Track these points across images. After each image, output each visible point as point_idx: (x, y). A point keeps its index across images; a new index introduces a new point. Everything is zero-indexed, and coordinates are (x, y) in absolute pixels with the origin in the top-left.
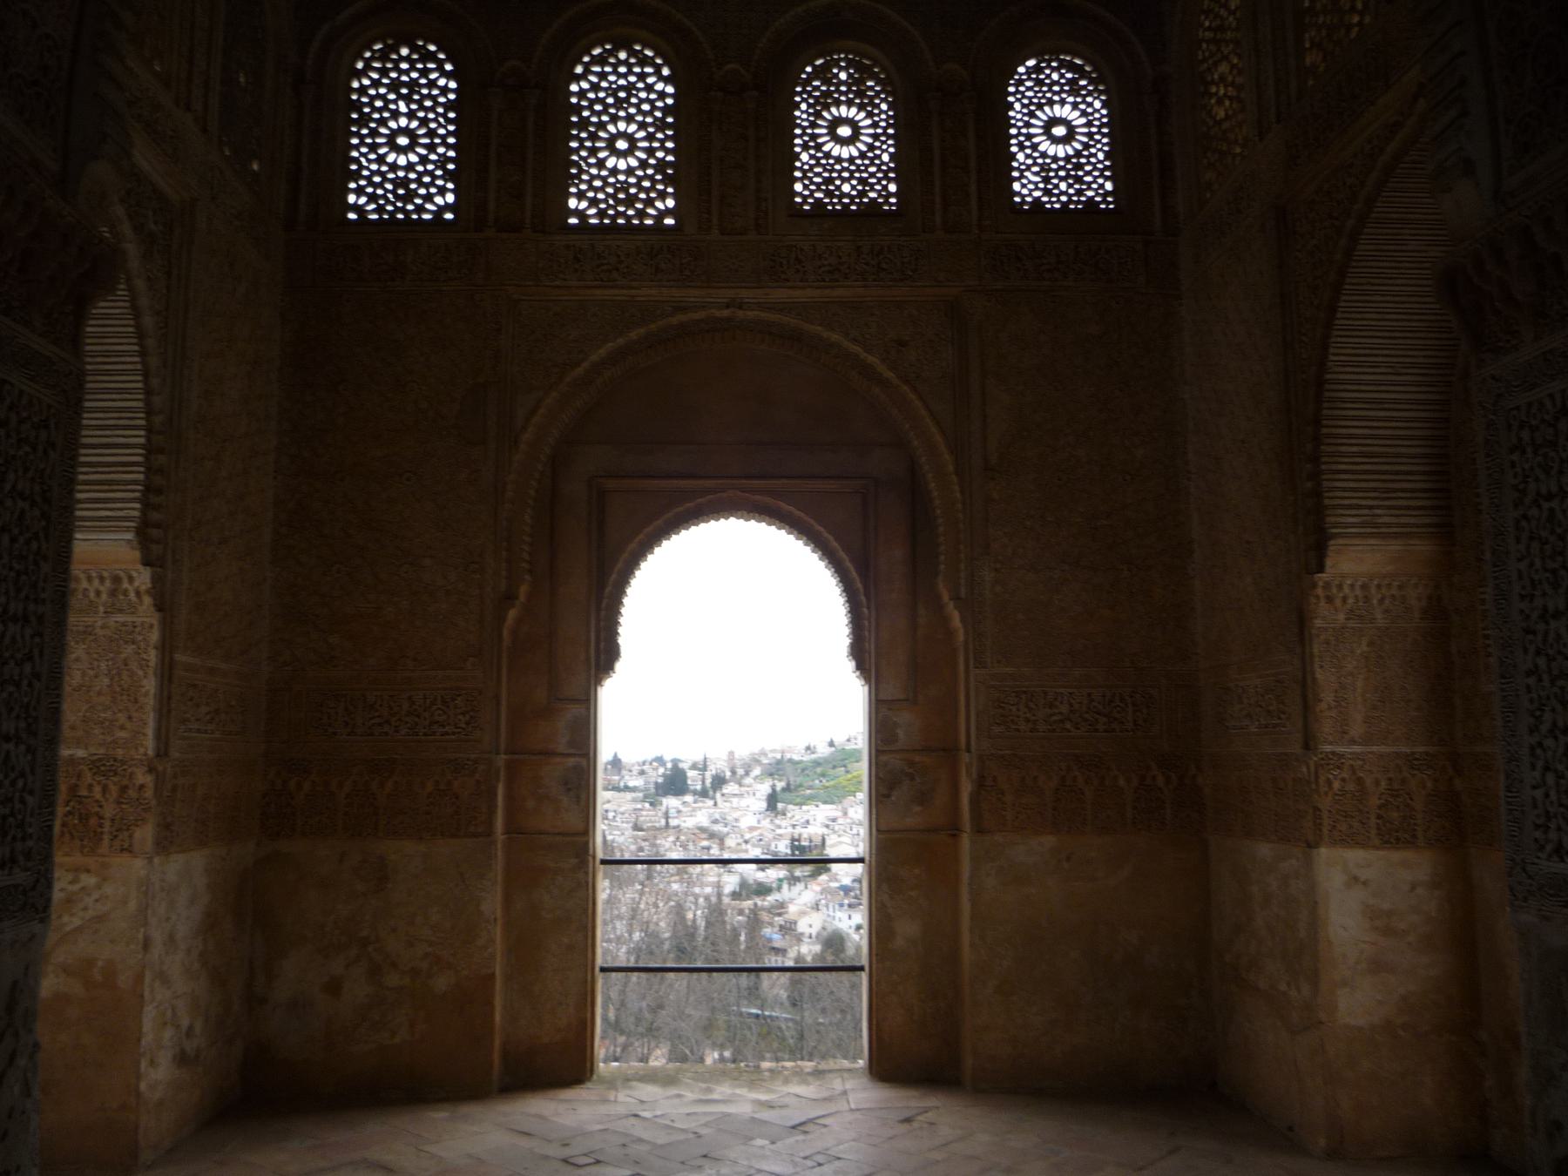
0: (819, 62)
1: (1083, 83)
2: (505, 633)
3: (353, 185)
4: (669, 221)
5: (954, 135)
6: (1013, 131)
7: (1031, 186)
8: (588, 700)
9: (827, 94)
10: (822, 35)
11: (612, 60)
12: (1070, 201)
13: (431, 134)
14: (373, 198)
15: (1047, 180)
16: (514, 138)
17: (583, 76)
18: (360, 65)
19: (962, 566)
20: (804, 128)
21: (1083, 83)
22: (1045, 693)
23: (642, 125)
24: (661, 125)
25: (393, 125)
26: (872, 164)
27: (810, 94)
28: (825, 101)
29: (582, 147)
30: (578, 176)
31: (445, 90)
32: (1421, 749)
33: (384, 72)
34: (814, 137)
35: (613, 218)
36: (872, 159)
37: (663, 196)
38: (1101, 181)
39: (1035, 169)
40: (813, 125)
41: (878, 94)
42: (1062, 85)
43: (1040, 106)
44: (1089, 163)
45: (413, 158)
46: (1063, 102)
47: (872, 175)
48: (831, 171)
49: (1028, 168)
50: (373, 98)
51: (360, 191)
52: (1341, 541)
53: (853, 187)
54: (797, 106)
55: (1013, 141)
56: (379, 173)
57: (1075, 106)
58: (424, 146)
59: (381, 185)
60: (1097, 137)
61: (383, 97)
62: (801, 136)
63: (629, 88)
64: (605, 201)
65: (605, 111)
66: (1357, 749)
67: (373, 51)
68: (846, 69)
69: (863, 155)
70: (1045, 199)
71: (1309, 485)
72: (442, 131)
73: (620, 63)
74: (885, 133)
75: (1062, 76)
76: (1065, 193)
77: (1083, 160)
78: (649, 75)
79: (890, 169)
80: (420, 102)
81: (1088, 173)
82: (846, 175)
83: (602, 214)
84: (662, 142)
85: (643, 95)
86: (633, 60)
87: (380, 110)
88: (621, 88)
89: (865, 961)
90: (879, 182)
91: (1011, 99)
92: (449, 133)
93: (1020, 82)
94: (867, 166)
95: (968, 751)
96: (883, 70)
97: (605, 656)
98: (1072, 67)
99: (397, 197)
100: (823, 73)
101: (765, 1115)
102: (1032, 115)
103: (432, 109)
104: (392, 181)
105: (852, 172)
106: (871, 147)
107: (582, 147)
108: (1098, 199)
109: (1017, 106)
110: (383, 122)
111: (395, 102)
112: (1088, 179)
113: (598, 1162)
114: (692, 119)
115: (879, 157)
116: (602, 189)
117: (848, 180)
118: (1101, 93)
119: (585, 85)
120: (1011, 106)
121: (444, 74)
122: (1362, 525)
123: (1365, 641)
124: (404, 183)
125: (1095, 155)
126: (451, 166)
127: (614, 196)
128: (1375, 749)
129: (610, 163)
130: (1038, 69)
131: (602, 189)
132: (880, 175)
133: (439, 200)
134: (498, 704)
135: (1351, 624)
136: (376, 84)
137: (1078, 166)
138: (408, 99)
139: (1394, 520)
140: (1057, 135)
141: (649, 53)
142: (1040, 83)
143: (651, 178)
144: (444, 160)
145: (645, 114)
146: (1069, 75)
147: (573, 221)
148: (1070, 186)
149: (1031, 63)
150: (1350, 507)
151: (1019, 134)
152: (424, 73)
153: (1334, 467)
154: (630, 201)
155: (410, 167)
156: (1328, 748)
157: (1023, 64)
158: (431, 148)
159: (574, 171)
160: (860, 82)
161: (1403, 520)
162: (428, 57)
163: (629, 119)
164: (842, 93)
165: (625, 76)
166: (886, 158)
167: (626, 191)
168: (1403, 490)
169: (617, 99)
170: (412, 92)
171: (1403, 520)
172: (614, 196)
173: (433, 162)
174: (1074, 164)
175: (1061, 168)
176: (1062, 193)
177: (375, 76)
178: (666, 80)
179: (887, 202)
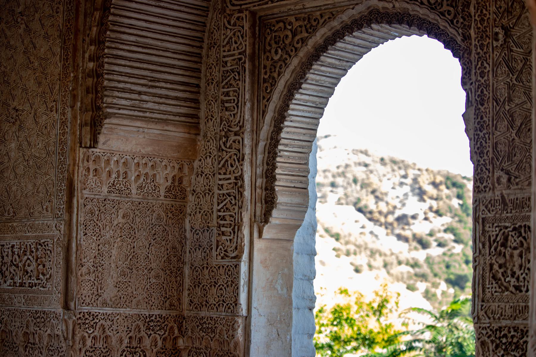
32: (157, 312)
52: (114, 121)
66: (109, 310)
71: (91, 65)
122: (133, 108)
123: (121, 213)
128: (122, 310)
135: (112, 197)
139: (157, 107)
150: (123, 90)
153: (115, 52)
156: (86, 309)
161: (163, 108)
168: (166, 81)
171: (163, 108)
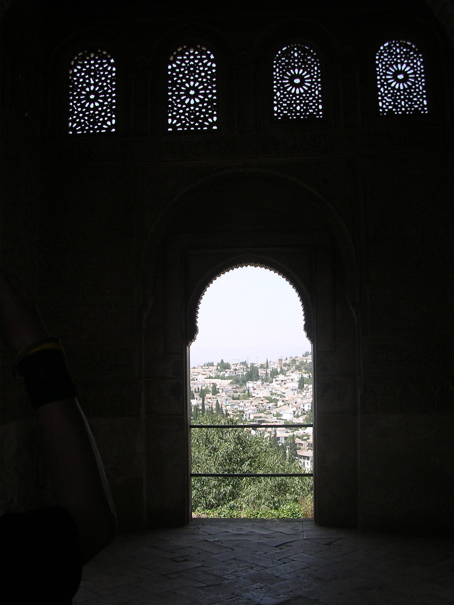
0: (284, 49)
1: (412, 53)
4: (215, 128)
5: (349, 82)
7: (387, 104)
9: (288, 64)
11: (187, 53)
12: (406, 110)
15: (395, 101)
16: (143, 92)
18: (73, 63)
20: (277, 81)
21: (412, 53)
23: (201, 83)
26: (311, 96)
28: (288, 67)
29: (173, 95)
30: (172, 108)
31: (111, 72)
33: (83, 66)
35: (189, 127)
36: (310, 94)
37: (211, 116)
38: (421, 100)
39: (389, 95)
40: (282, 79)
42: (402, 55)
43: (391, 65)
44: (415, 92)
45: (97, 104)
46: (402, 63)
48: (291, 101)
49: (386, 95)
50: (79, 78)
53: (301, 108)
54: (274, 70)
55: (379, 82)
56: (81, 112)
57: (408, 65)
60: (419, 79)
62: (276, 84)
63: (195, 66)
64: (184, 119)
65: (184, 77)
67: (78, 57)
68: (297, 51)
69: (306, 92)
70: (394, 110)
72: (110, 91)
74: (316, 81)
75: (401, 50)
77: (412, 91)
80: (100, 78)
81: (416, 97)
82: (298, 102)
83: (183, 126)
84: (211, 90)
85: (201, 69)
88: (191, 66)
90: (314, 105)
91: (377, 62)
92: (113, 92)
93: (382, 54)
94: (308, 97)
97: (191, 332)
98: (406, 46)
99: (90, 123)
100: (286, 54)
101: (264, 540)
105: (301, 101)
106: (310, 88)
108: (420, 109)
109: (380, 65)
110: (83, 89)
111: (89, 79)
112: (415, 99)
113: (186, 560)
114: (223, 78)
115: (314, 92)
116: (183, 114)
117: (299, 104)
118: (420, 58)
119: (174, 66)
120: (377, 66)
124: (93, 116)
125: (418, 88)
126: (114, 107)
127: (189, 117)
129: (187, 101)
130: (389, 47)
131: (183, 114)
132: (314, 101)
137: (410, 93)
138: (94, 77)
140: (400, 78)
142: (390, 54)
143: (206, 108)
145: (203, 77)
146: (405, 50)
147: (170, 129)
148: (406, 103)
149: (386, 45)
151: (381, 79)
154: (196, 119)
155: (95, 108)
158: (105, 99)
159: (170, 106)
160: (304, 57)
163: (195, 80)
164: (295, 63)
165: (193, 60)
166: (317, 93)
167: (194, 114)
169: (189, 71)
172: (189, 117)
173: (106, 106)
175: (401, 95)
176: (402, 107)
177: (79, 67)
178: (212, 61)
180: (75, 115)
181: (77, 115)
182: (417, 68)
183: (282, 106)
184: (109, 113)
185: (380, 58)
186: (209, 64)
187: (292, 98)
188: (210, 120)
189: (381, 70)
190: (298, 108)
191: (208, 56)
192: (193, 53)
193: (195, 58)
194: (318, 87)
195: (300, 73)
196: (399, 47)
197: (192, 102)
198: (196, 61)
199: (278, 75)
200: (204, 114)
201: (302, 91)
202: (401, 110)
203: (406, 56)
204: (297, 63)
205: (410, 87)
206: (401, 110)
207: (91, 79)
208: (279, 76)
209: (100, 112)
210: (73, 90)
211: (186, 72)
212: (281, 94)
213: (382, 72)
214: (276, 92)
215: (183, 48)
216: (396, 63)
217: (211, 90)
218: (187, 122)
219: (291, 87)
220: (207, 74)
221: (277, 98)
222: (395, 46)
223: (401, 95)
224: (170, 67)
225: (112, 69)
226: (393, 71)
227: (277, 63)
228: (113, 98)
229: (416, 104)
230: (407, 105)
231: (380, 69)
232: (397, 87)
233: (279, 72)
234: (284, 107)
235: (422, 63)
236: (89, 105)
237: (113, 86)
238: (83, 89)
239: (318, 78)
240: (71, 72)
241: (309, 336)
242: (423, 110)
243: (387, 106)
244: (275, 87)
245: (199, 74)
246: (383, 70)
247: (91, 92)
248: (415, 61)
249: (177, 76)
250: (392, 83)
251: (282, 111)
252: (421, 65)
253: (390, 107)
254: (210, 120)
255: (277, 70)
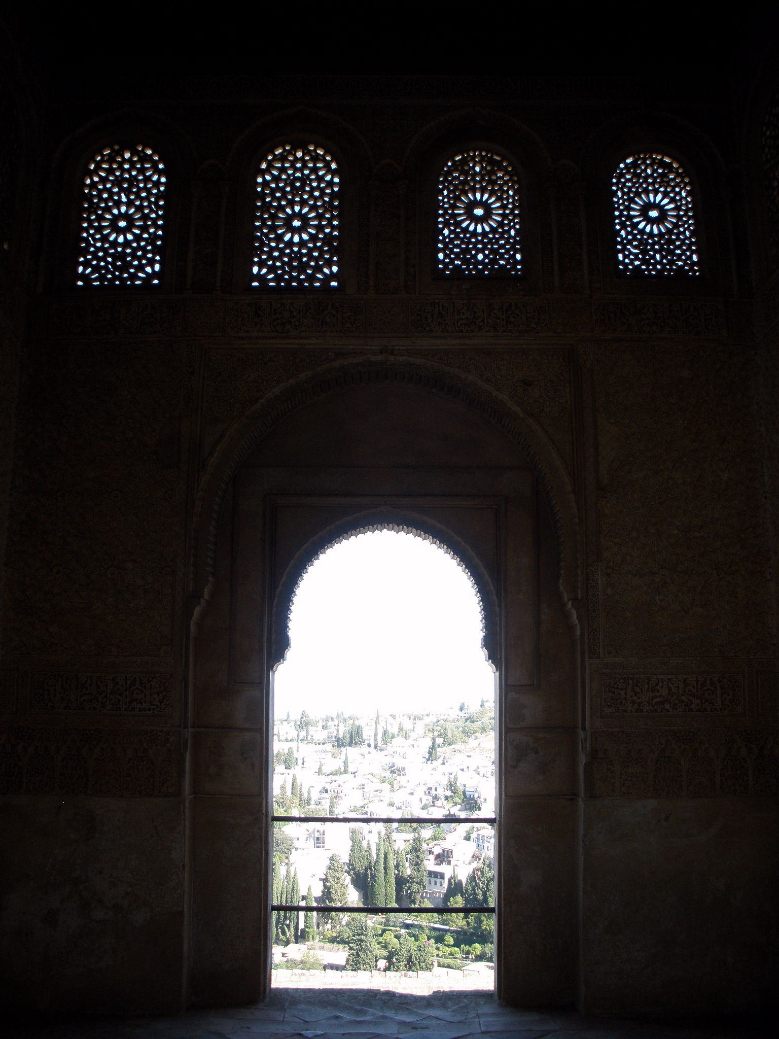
0: (457, 159)
1: (671, 177)
2: (193, 627)
3: (82, 259)
5: (567, 215)
6: (617, 213)
7: (632, 257)
8: (261, 683)
9: (465, 182)
10: (461, 137)
13: (145, 217)
14: (96, 269)
15: (644, 252)
17: (268, 170)
19: (579, 571)
20: (446, 210)
22: (649, 680)
23: (313, 208)
24: (329, 207)
25: (115, 211)
26: (502, 238)
27: (450, 183)
31: (157, 184)
34: (454, 216)
40: (454, 207)
41: (506, 183)
43: (638, 194)
44: (678, 239)
45: (130, 237)
46: (656, 192)
47: (502, 247)
48: (468, 245)
51: (86, 264)
53: (485, 256)
56: (102, 249)
57: (665, 194)
58: (138, 227)
59: (103, 259)
61: (109, 191)
62: (443, 216)
63: (304, 180)
68: (480, 162)
70: (644, 267)
73: (296, 160)
75: (654, 171)
76: (660, 263)
78: (320, 169)
79: (516, 242)
81: (679, 247)
83: (278, 278)
85: (315, 184)
86: (307, 158)
87: (106, 201)
88: (298, 179)
89: (492, 903)
90: (507, 252)
91: (614, 188)
92: (159, 217)
93: (622, 175)
94: (497, 240)
95: (584, 729)
96: (510, 164)
98: (662, 164)
100: (461, 167)
102: (632, 200)
103: (147, 198)
104: (111, 255)
105: (485, 245)
107: (264, 224)
109: (619, 194)
110: (108, 209)
111: (118, 194)
112: (678, 252)
114: (352, 202)
115: (509, 231)
116: (279, 258)
117: (482, 251)
118: (686, 184)
119: (268, 178)
121: (156, 171)
124: (123, 255)
125: (684, 233)
126: (159, 243)
127: (289, 264)
129: (287, 237)
130: (634, 165)
131: (279, 258)
133: (149, 269)
134: (186, 686)
136: (104, 180)
137: (672, 242)
138: (128, 192)
141: (320, 152)
142: (638, 176)
143: (320, 249)
144: (154, 237)
145: (316, 199)
146: (660, 171)
147: (255, 284)
148: (662, 257)
149: (628, 161)
151: (621, 215)
152: (142, 171)
155: (127, 243)
157: (624, 161)
158: (144, 229)
162: (144, 158)
163: (303, 203)
165: (301, 170)
166: (513, 232)
170: (131, 186)
174: (666, 241)
176: (657, 263)
178: (334, 173)
179: (514, 268)
180: (91, 253)
181: (94, 254)
182: (680, 200)
183: (452, 252)
184: (149, 252)
185: (619, 182)
186: (328, 178)
187: (469, 239)
188: (326, 271)
189: (621, 201)
190: (480, 257)
191: (327, 165)
192: (302, 159)
193: (305, 166)
194: (515, 224)
195: (484, 199)
196: (651, 165)
197: (296, 239)
198: (306, 172)
199: (446, 200)
200: (316, 259)
201: (487, 229)
202: (655, 269)
203: (662, 181)
204: (480, 182)
205: (669, 232)
206: (655, 269)
207: (123, 195)
208: (448, 202)
209: (135, 250)
210: (90, 211)
211: (288, 189)
212: (451, 232)
213: (623, 204)
214: (443, 229)
215: (285, 150)
216: (647, 192)
217: (330, 221)
218: (285, 272)
219: (468, 222)
220: (323, 194)
221: (445, 238)
222: (644, 162)
223: (655, 243)
224: (260, 180)
225: (159, 179)
226: (641, 203)
227: (446, 180)
228: (157, 227)
229: (679, 259)
230: (665, 261)
231: (619, 199)
232: (648, 229)
233: (448, 196)
234: (457, 254)
235: (689, 193)
236: (116, 239)
237: (159, 207)
238: (108, 209)
239: (515, 207)
240: (88, 182)
241: (493, 657)
242: (692, 269)
243: (632, 261)
244: (440, 219)
245: (311, 193)
246: (624, 201)
247: (121, 216)
248: (677, 190)
249: (272, 194)
250: (639, 223)
251: (452, 261)
252: (687, 196)
253: (637, 263)
254: (326, 271)
255: (445, 192)
